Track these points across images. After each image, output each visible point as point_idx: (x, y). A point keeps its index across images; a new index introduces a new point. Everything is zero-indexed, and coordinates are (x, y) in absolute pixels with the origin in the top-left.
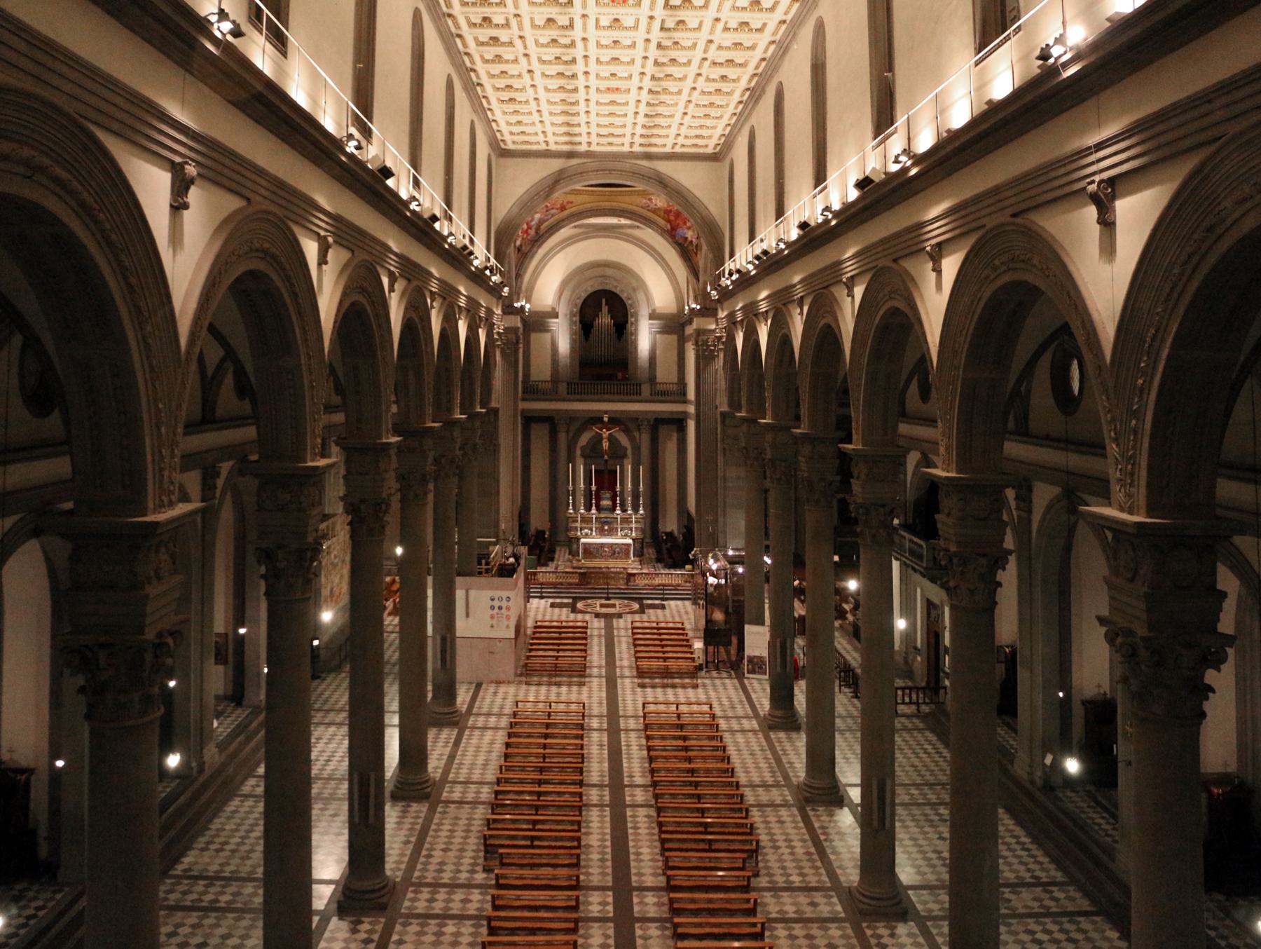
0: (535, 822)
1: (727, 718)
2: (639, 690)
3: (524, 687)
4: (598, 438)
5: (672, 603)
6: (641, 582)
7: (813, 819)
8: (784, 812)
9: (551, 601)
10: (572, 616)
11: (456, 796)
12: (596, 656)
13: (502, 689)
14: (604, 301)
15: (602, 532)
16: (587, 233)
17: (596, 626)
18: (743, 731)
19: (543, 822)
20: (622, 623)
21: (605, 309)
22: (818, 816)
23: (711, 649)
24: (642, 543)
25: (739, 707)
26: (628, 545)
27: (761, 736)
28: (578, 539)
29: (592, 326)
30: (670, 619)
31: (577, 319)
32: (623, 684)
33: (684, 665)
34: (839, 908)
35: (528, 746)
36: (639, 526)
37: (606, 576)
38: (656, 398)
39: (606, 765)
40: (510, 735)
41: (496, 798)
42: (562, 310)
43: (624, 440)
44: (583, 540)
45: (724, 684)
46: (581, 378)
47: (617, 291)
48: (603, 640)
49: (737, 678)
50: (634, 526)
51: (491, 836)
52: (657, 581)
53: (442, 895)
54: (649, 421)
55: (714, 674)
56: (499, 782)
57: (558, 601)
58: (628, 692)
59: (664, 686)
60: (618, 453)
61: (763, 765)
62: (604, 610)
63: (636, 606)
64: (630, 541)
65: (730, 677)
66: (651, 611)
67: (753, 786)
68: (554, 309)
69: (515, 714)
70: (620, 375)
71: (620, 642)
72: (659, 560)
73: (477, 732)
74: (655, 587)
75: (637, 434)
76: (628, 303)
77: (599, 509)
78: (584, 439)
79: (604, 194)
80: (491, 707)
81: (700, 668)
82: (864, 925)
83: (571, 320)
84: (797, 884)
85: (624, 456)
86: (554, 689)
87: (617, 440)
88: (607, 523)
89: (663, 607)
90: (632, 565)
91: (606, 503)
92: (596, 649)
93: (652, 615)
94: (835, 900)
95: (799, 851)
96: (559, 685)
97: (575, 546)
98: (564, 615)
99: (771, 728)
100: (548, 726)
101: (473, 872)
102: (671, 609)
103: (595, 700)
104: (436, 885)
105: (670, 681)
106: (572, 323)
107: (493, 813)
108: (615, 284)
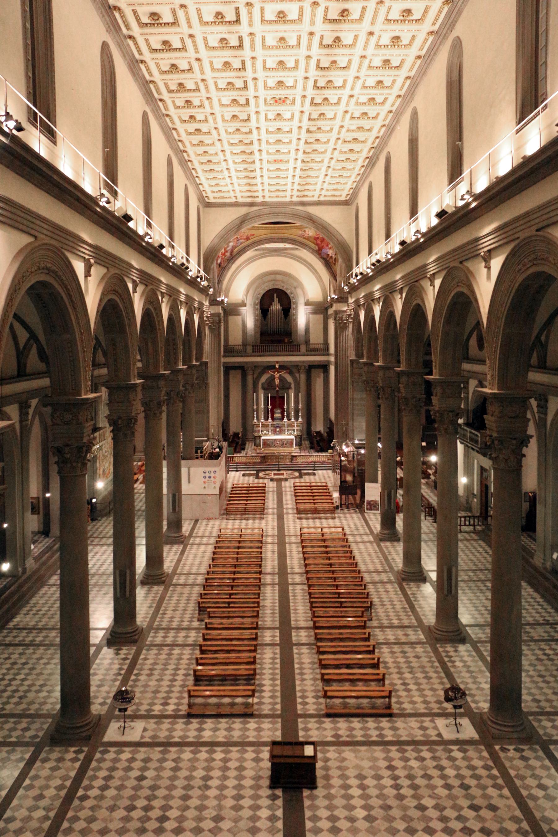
0: (231, 594)
1: (353, 535)
2: (298, 521)
3: (225, 521)
4: (273, 378)
5: (320, 472)
6: (300, 460)
7: (407, 589)
8: (389, 586)
9: (243, 472)
10: (256, 481)
11: (182, 581)
12: (271, 502)
13: (211, 523)
14: (275, 295)
15: (275, 432)
16: (264, 254)
17: (271, 486)
18: (363, 542)
19: (236, 594)
20: (287, 484)
21: (276, 300)
22: (410, 588)
23: (344, 497)
24: (301, 438)
25: (361, 528)
26: (292, 439)
27: (375, 544)
28: (260, 437)
29: (268, 311)
30: (318, 481)
31: (258, 307)
32: (287, 518)
33: (326, 506)
34: (422, 637)
35: (227, 553)
36: (298, 428)
37: (278, 457)
38: (309, 353)
39: (276, 562)
40: (215, 548)
41: (206, 582)
42: (249, 301)
43: (289, 378)
44: (263, 438)
45: (352, 517)
46: (261, 343)
47: (284, 289)
48: (275, 493)
49: (360, 513)
50: (295, 428)
51: (203, 602)
52: (311, 459)
53: (172, 634)
54: (305, 367)
55: (346, 511)
56: (208, 573)
57: (247, 472)
58: (291, 522)
59: (314, 518)
60: (285, 386)
61: (376, 561)
62: (276, 477)
63: (297, 474)
64: (293, 437)
65: (356, 512)
66: (307, 477)
67: (369, 572)
68: (243, 301)
69: (219, 536)
70: (286, 340)
71: (286, 494)
72: (311, 448)
73: (195, 547)
74: (309, 463)
75: (297, 375)
76: (291, 296)
77: (273, 419)
78: (264, 378)
79: (271, 229)
80: (204, 532)
81: (337, 507)
82: (438, 646)
83: (254, 307)
84: (396, 625)
85: (290, 388)
86: (244, 522)
87: (284, 378)
88: (278, 427)
89: (314, 474)
90: (295, 450)
91: (278, 415)
92: (271, 499)
93: (307, 479)
94: (420, 632)
95: (398, 607)
96: (247, 519)
97: (258, 441)
98: (251, 480)
99: (381, 540)
100: (240, 543)
101: (191, 621)
102: (319, 475)
103: (270, 527)
104: (168, 629)
105: (318, 515)
106: (255, 309)
107: (204, 590)
108: (283, 285)
